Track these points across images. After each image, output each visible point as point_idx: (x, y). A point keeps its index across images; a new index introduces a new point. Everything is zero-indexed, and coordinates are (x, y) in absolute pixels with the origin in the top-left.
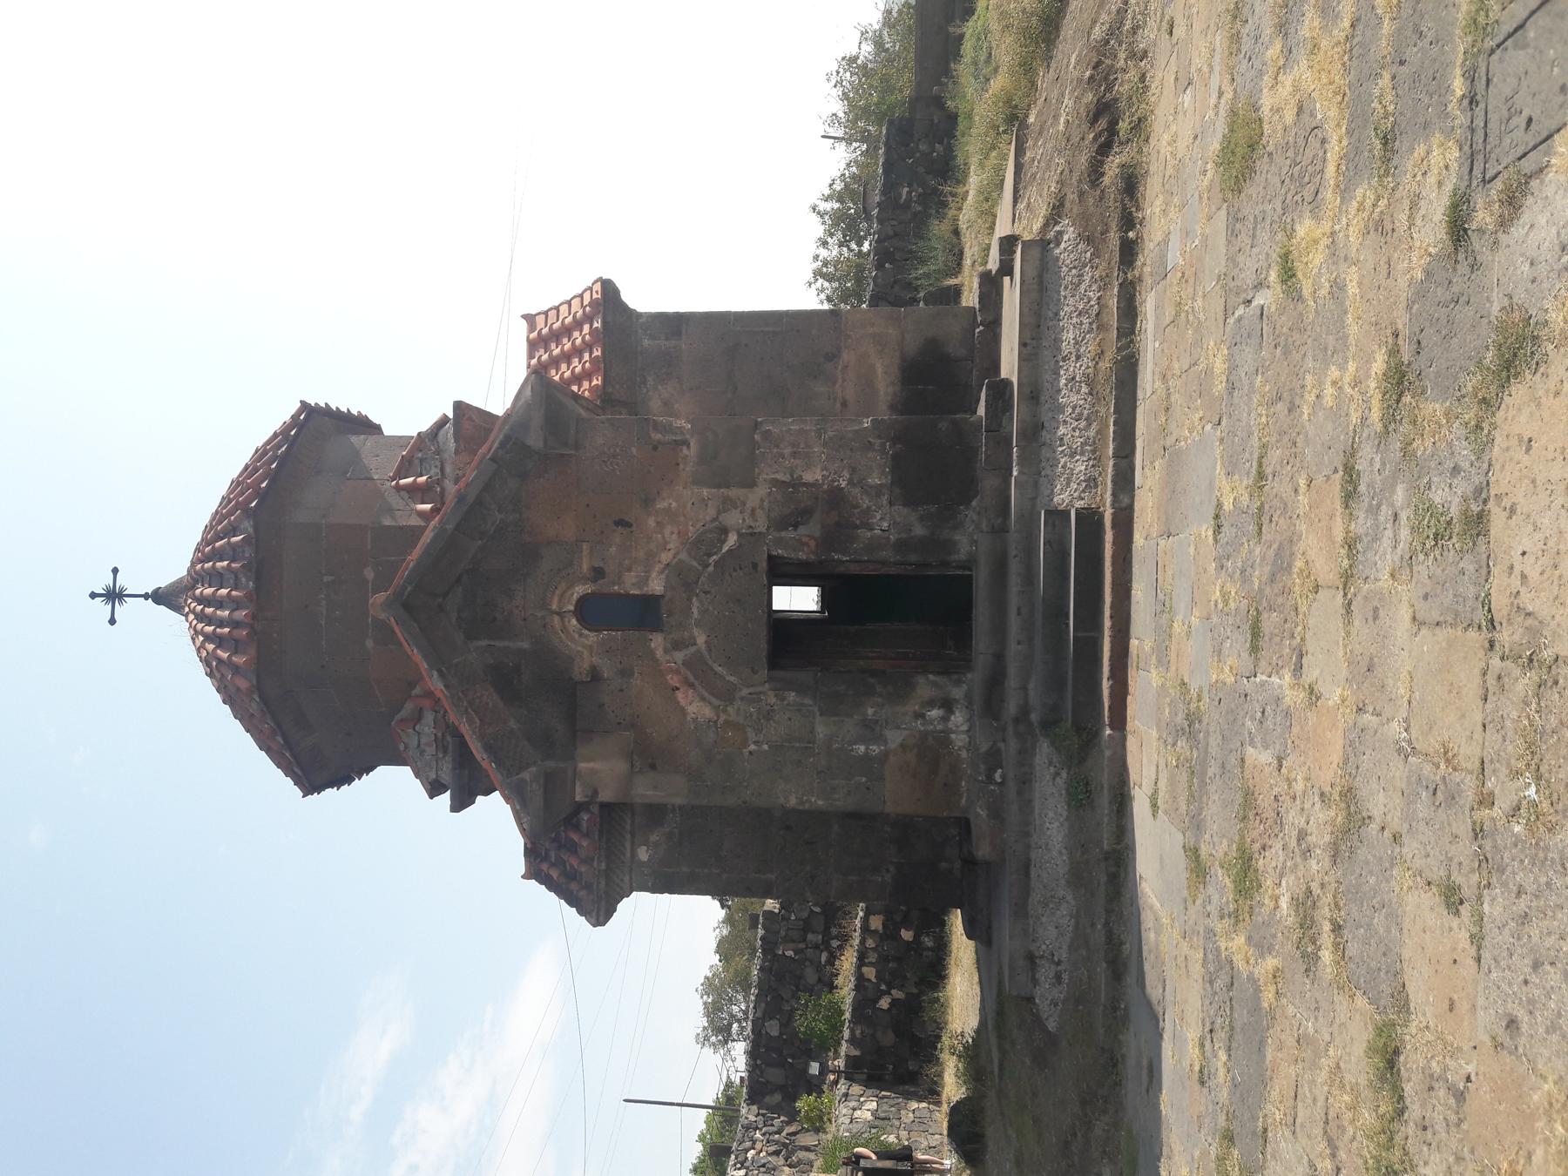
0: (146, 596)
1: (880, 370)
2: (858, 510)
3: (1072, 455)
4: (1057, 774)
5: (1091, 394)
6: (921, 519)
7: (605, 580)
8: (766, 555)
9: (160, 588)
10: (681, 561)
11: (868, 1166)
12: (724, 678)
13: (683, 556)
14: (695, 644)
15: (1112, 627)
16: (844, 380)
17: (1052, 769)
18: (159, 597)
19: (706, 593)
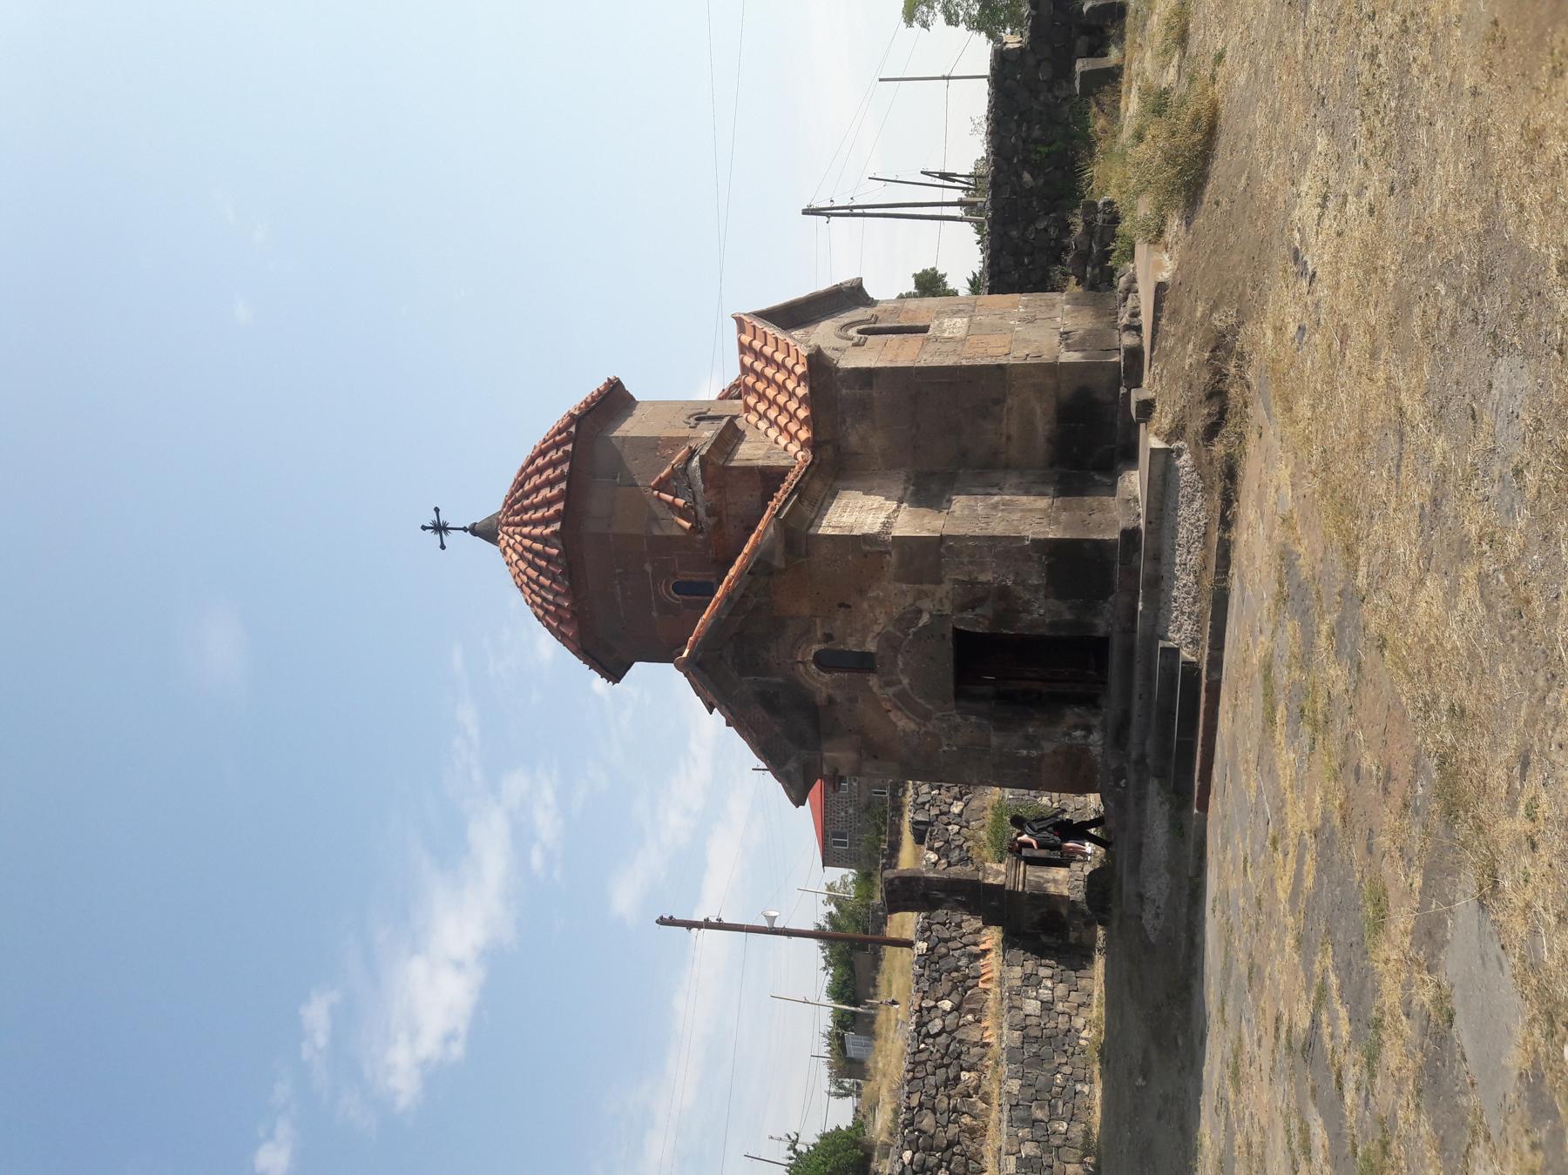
0: (465, 529)
1: (1038, 411)
3: (1183, 613)
4: (1162, 803)
5: (1197, 583)
8: (951, 630)
9: (476, 524)
10: (888, 631)
11: (1028, 855)
13: (890, 628)
14: (901, 683)
15: (1203, 751)
16: (1008, 420)
17: (1159, 798)
18: (474, 530)
19: (908, 652)
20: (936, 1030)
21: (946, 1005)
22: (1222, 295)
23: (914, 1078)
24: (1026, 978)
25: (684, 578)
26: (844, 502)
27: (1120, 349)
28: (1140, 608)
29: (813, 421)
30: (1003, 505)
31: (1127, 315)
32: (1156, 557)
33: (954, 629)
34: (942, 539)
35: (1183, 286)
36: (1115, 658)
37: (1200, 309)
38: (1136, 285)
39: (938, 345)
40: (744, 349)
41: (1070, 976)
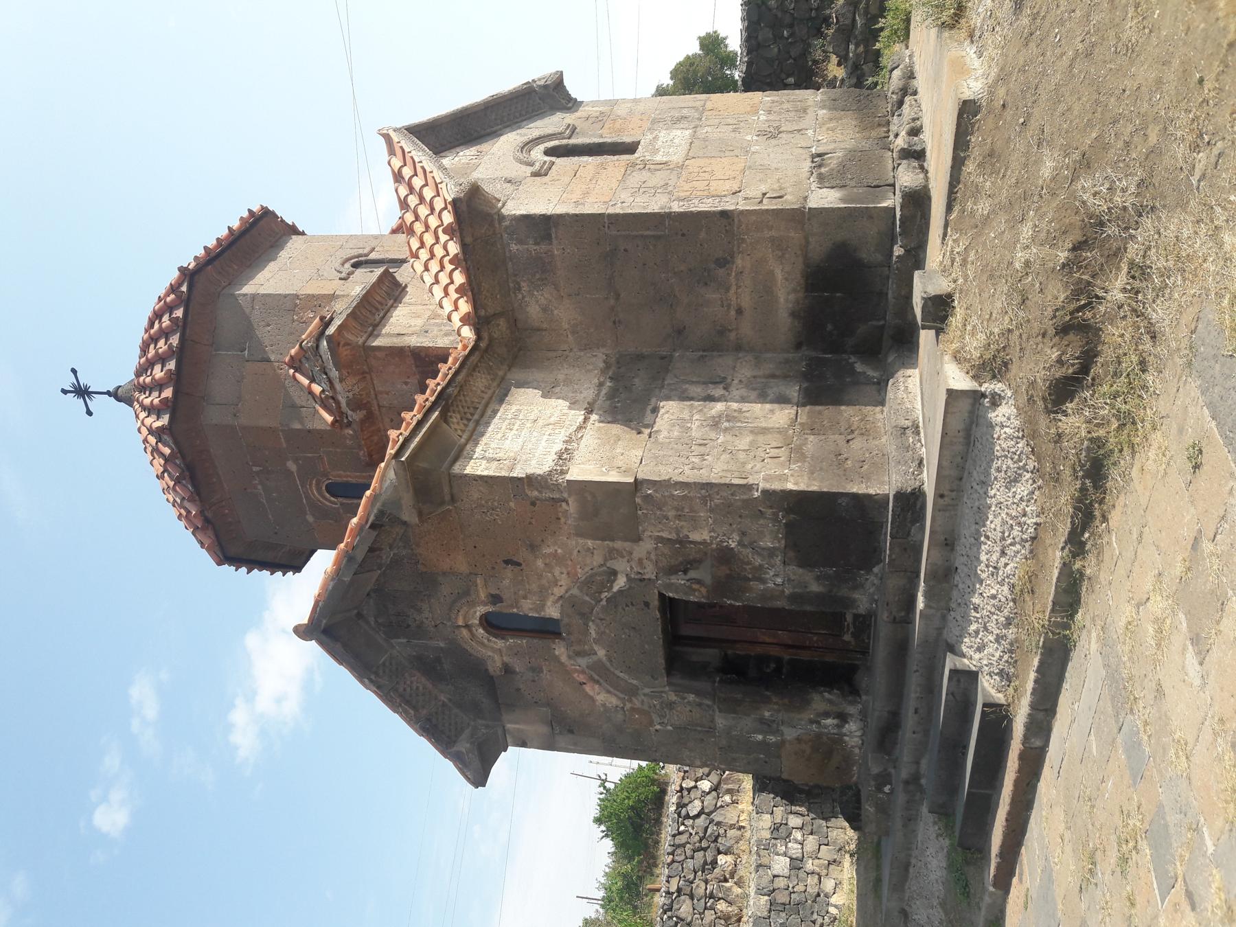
0: (108, 393)
2: (750, 566)
5: (1014, 601)
6: (818, 578)
7: (504, 604)
8: (657, 597)
12: (626, 681)
13: (575, 591)
14: (596, 654)
16: (738, 287)
19: (601, 620)
20: (695, 812)
21: (705, 785)
22: (1101, 145)
23: (673, 861)
24: (776, 828)
25: (339, 480)
26: (514, 408)
27: (893, 185)
28: (920, 603)
29: (472, 291)
30: (728, 421)
31: (903, 133)
32: (948, 543)
33: (661, 595)
34: (638, 484)
35: (1009, 113)
36: (881, 653)
37: (1049, 164)
38: (915, 83)
39: (645, 175)
40: (398, 177)
41: (820, 826)
